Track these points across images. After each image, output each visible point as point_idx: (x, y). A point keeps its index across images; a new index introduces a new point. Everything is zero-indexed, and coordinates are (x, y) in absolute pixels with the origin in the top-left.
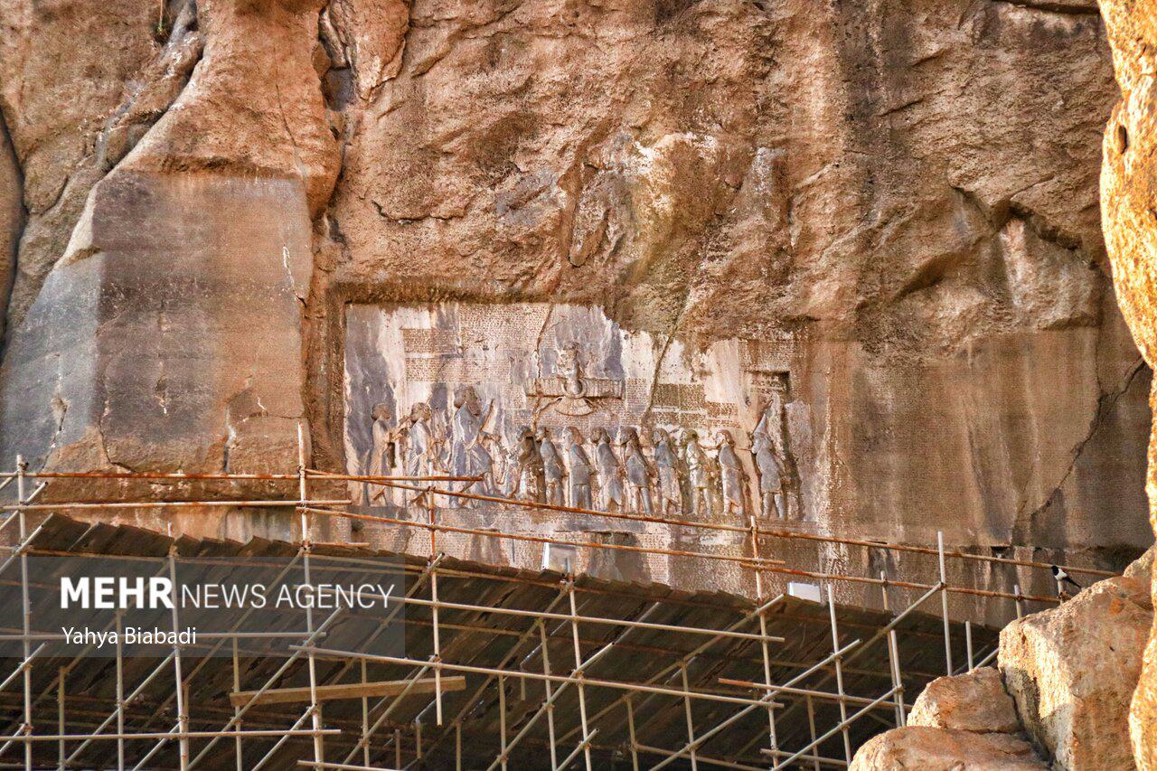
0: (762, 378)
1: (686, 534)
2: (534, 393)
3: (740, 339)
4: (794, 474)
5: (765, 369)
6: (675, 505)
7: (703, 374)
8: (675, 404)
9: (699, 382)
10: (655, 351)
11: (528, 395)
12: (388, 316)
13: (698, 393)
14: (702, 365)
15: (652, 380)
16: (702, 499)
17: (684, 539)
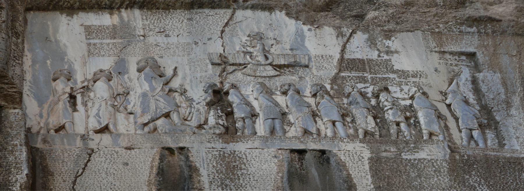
0: (448, 56)
1: (386, 151)
2: (219, 62)
3: (423, 31)
5: (450, 50)
7: (389, 52)
8: (364, 70)
9: (386, 57)
10: (340, 38)
11: (213, 64)
12: (69, 18)
13: (388, 67)
14: (388, 47)
15: (338, 56)
16: (399, 131)
17: (384, 154)
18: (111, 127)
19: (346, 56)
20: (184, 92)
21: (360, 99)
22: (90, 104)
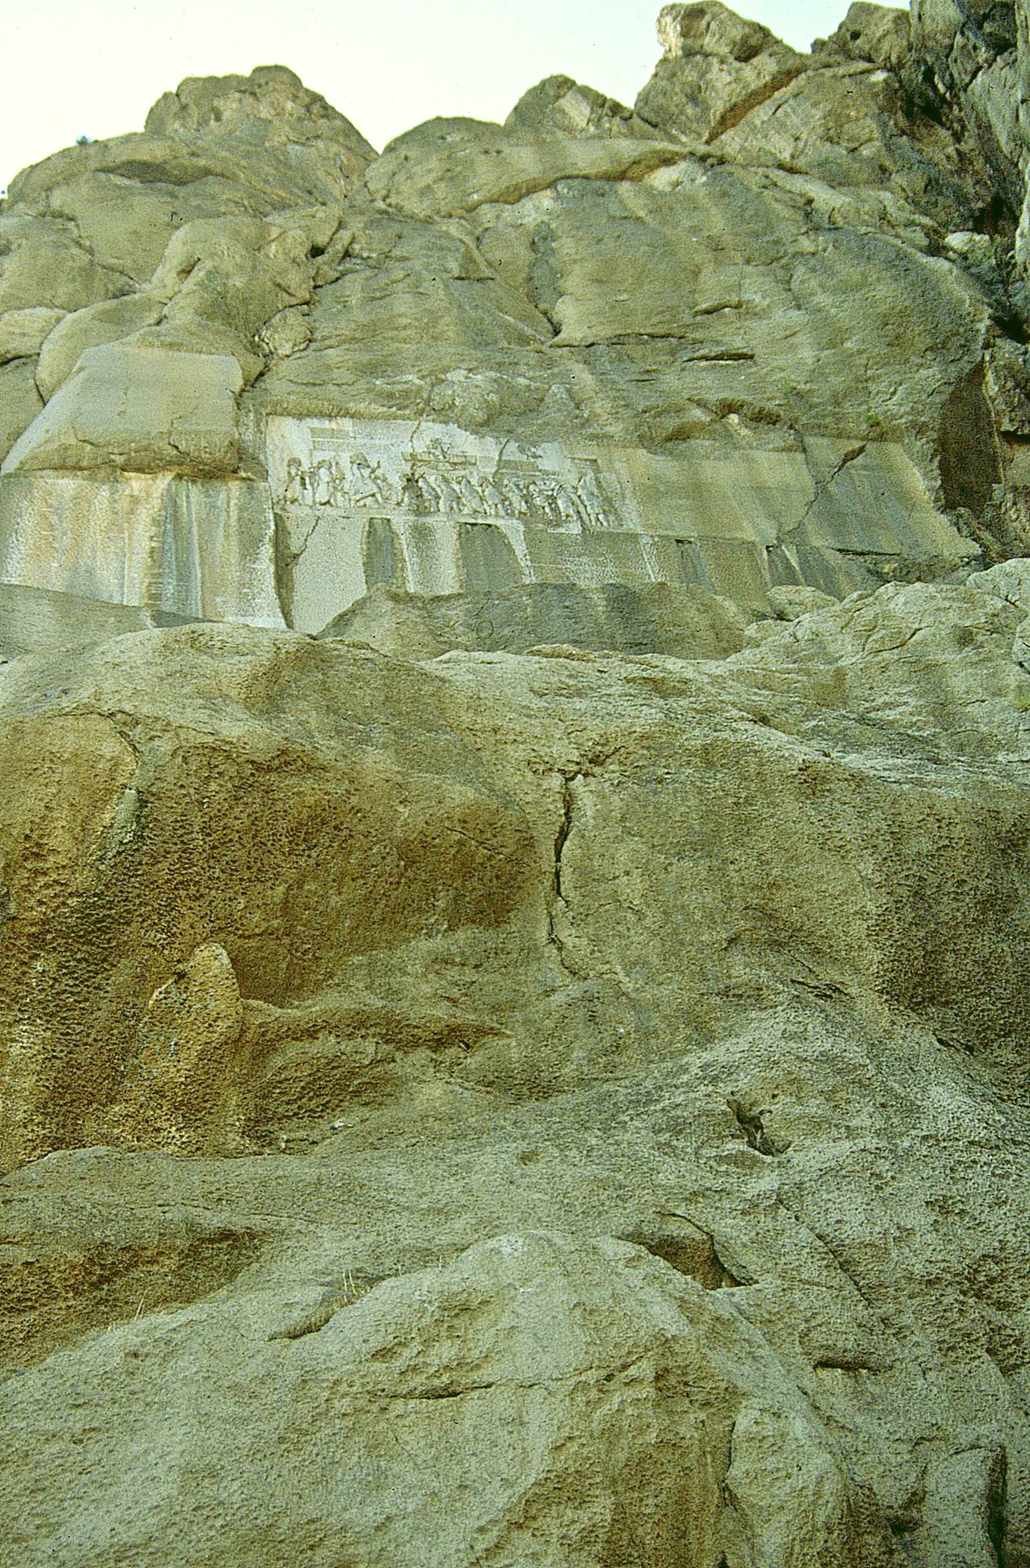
4: (611, 505)
6: (525, 514)
7: (535, 456)
15: (497, 458)
18: (332, 501)
19: (504, 458)
20: (385, 480)
21: (514, 488)
22: (316, 485)
